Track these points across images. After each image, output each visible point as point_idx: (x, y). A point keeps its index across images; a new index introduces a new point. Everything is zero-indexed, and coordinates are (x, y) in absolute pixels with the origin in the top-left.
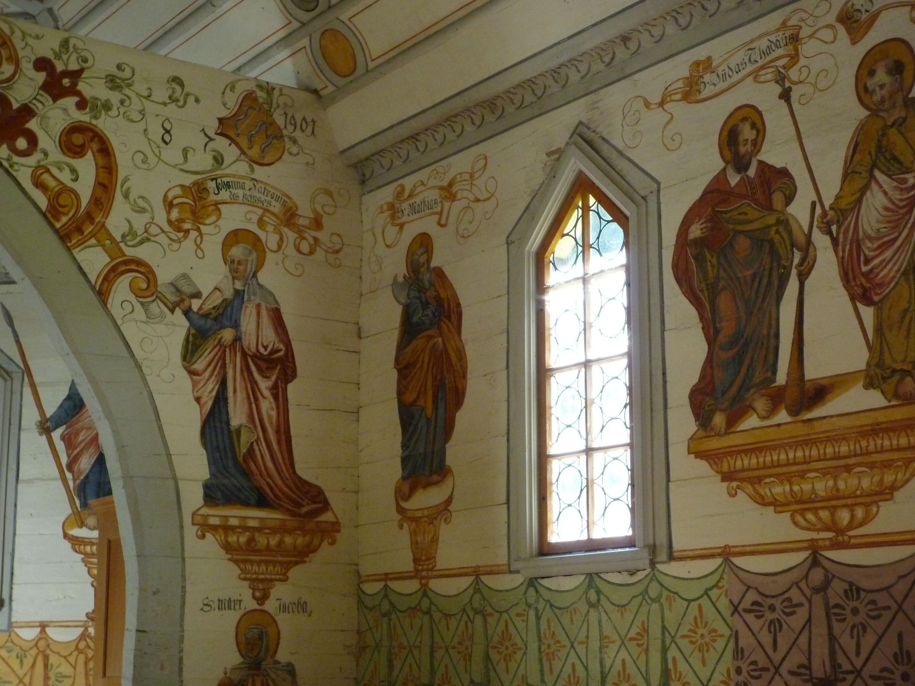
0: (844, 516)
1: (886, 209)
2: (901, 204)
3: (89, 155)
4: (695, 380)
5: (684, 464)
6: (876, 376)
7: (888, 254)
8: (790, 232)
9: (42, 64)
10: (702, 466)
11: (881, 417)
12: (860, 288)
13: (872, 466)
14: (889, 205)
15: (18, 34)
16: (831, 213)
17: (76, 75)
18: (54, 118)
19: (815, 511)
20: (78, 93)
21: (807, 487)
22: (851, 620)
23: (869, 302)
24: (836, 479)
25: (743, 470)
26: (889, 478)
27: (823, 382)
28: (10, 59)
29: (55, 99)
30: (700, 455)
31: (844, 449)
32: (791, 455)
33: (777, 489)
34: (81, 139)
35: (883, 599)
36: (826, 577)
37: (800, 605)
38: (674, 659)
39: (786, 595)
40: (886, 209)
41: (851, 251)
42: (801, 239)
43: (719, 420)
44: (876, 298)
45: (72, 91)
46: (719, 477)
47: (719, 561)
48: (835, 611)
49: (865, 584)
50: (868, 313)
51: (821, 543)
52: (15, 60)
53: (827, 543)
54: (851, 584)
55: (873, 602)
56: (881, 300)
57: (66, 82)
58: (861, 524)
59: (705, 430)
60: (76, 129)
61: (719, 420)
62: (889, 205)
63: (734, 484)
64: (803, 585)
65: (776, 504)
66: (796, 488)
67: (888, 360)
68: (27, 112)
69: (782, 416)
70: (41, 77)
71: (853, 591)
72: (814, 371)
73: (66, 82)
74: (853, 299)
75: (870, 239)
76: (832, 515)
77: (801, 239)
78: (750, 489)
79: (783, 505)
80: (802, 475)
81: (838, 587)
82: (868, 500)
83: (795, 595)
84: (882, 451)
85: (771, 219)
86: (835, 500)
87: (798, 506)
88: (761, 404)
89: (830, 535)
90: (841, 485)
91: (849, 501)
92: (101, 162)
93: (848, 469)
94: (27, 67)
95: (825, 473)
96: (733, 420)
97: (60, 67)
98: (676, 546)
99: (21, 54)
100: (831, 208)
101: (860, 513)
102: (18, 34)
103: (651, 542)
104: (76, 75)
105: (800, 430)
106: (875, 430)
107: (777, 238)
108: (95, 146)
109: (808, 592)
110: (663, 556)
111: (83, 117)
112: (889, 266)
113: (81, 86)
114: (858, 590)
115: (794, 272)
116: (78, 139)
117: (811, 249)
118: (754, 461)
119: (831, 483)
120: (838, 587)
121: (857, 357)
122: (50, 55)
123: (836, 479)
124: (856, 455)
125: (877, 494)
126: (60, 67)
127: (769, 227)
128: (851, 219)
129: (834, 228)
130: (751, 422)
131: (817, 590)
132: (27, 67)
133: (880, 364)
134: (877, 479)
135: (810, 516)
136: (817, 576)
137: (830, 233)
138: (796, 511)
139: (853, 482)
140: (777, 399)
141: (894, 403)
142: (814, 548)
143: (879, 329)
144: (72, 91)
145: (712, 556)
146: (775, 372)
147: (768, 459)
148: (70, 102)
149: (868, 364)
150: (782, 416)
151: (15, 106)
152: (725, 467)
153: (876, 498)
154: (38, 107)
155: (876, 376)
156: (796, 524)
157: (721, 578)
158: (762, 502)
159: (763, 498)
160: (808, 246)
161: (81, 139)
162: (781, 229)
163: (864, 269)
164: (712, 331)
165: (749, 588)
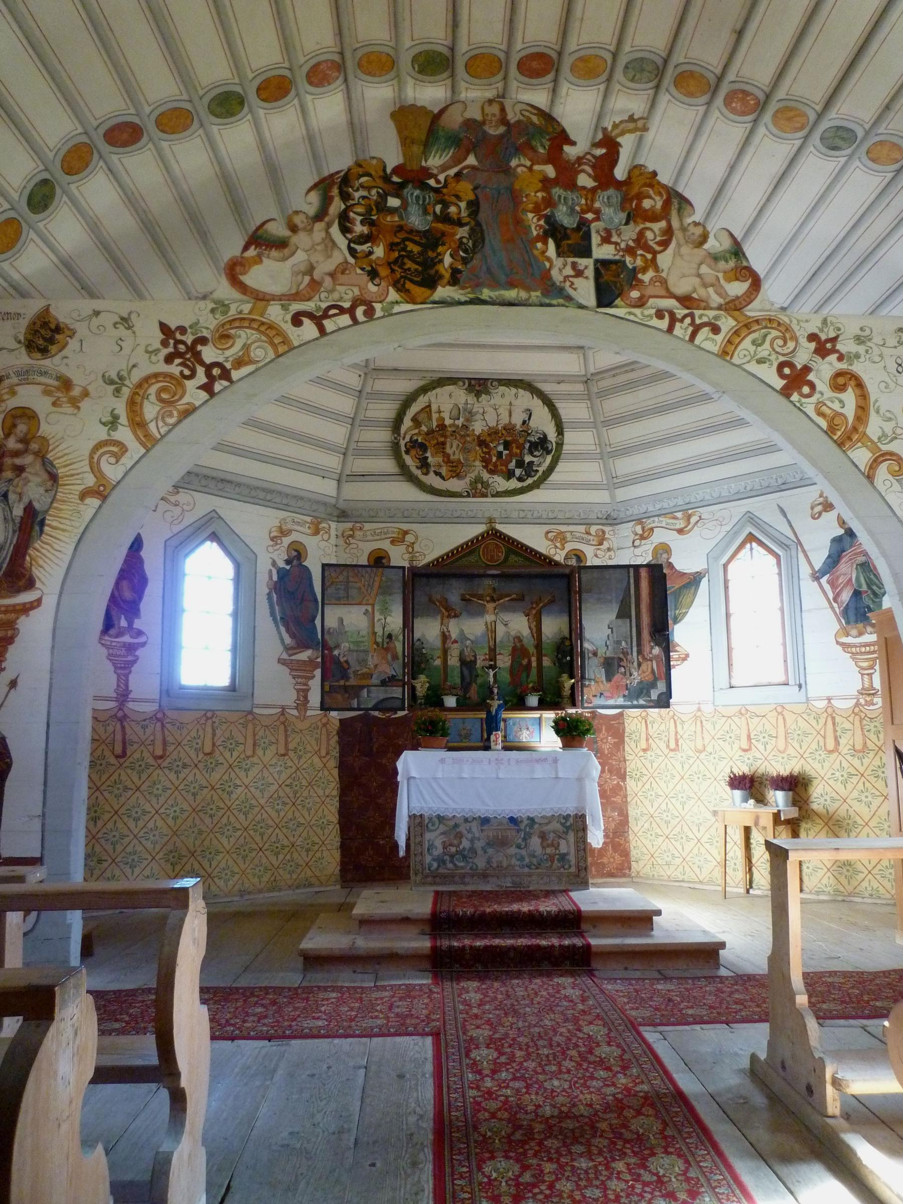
3: (850, 390)
9: (812, 337)
15: (795, 322)
17: (834, 340)
18: (824, 371)
20: (837, 351)
28: (791, 338)
29: (823, 358)
34: (844, 380)
45: (834, 351)
52: (795, 338)
57: (829, 346)
60: (839, 374)
68: (807, 369)
70: (813, 345)
73: (829, 346)
92: (858, 392)
94: (803, 341)
97: (823, 337)
99: (798, 334)
102: (795, 322)
104: (834, 340)
108: (853, 383)
111: (843, 366)
113: (838, 347)
116: (841, 380)
122: (816, 331)
126: (823, 337)
132: (803, 341)
144: (834, 351)
148: (833, 358)
151: (799, 367)
154: (813, 365)
161: (844, 380)
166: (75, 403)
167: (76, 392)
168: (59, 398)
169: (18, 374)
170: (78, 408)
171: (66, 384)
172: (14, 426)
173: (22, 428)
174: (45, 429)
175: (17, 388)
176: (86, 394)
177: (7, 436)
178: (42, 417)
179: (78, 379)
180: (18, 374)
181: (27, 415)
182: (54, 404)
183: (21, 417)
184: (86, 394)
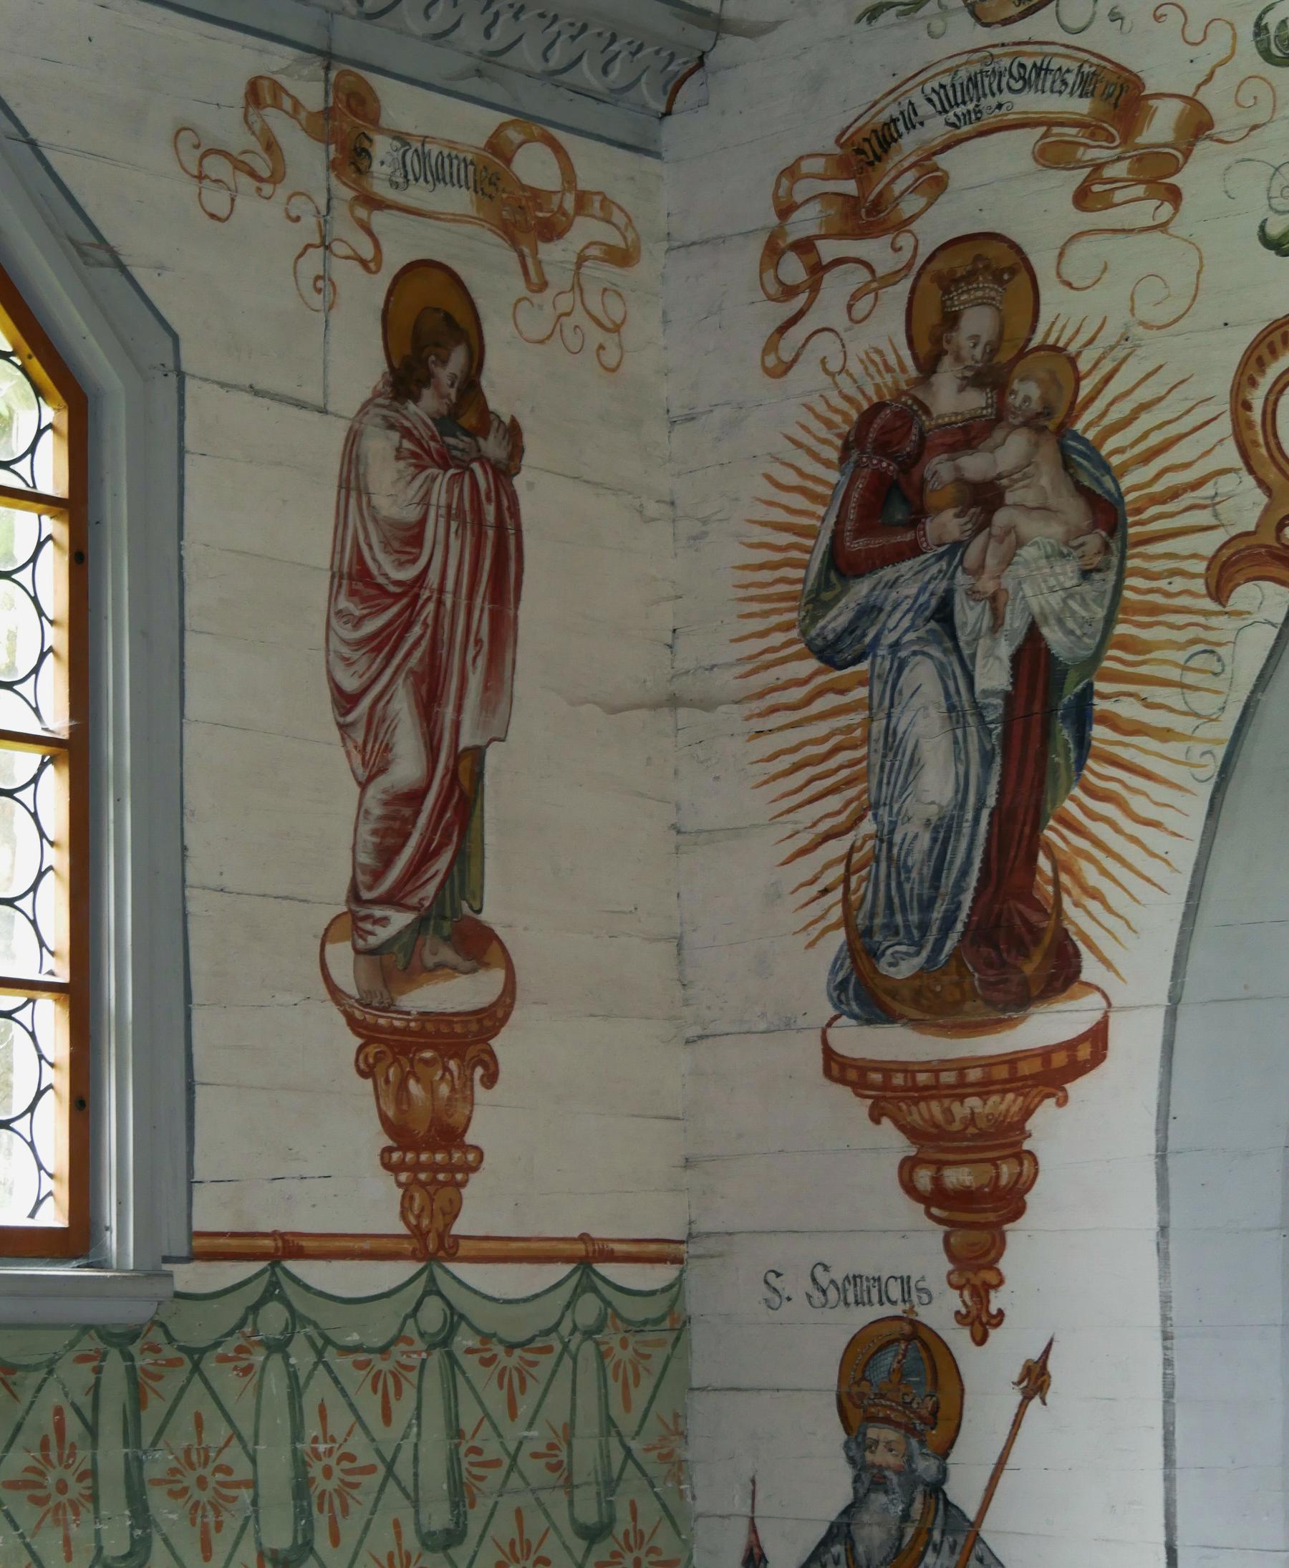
166: (1159, 175)
167: (1160, 127)
168: (1098, 167)
169: (944, 101)
170: (1174, 195)
171: (1121, 97)
172: (951, 320)
173: (977, 322)
174: (1063, 315)
175: (943, 161)
176: (1198, 125)
177: (928, 367)
178: (1043, 263)
179: (1163, 67)
180: (944, 101)
181: (991, 264)
182: (1083, 198)
183: (970, 276)
184: (1198, 125)
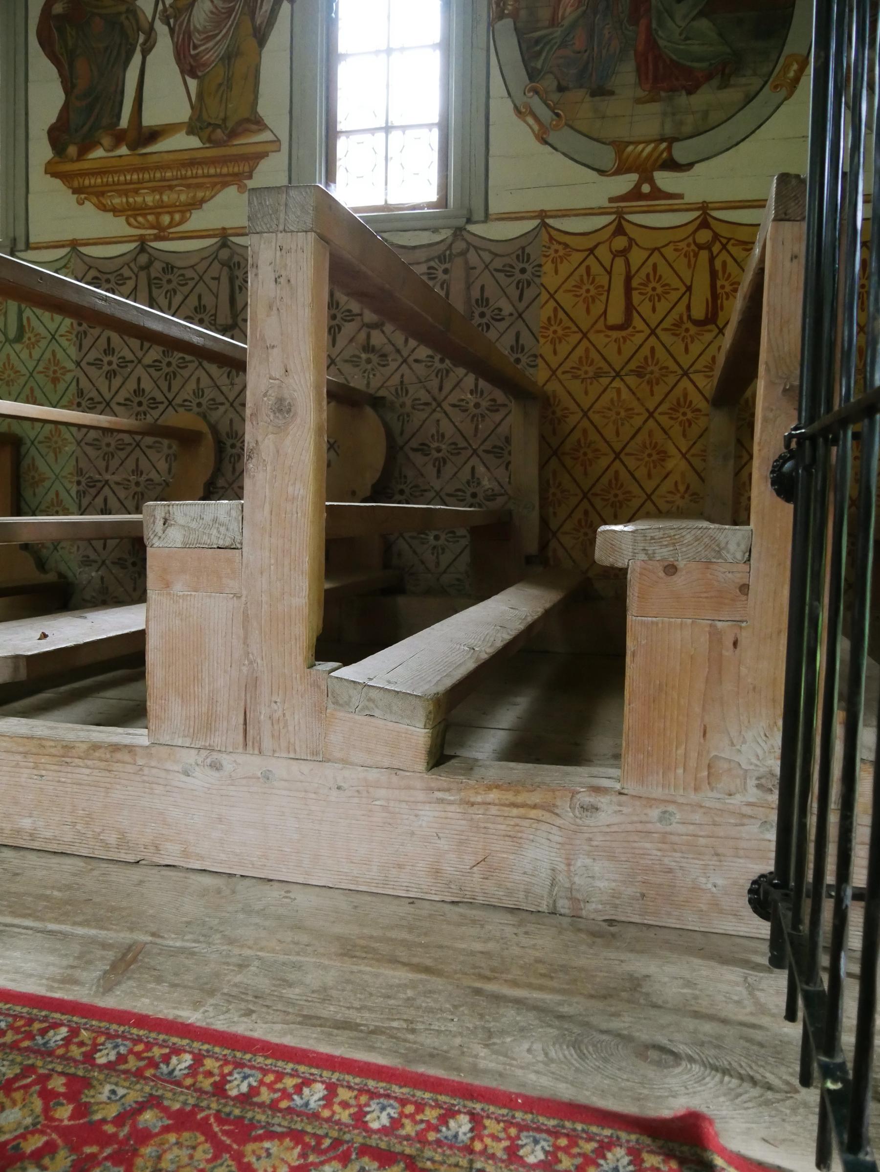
0: (166, 219)
1: (212, 12)
2: (223, 11)
4: (54, 120)
5: (39, 180)
6: (196, 126)
7: (210, 44)
8: (137, 21)
10: (57, 182)
11: (198, 155)
12: (188, 65)
13: (188, 186)
14: (214, 10)
16: (170, 11)
19: (144, 216)
21: (139, 199)
22: (167, 287)
23: (194, 75)
24: (161, 194)
25: (90, 186)
26: (200, 194)
27: (156, 128)
30: (55, 175)
31: (169, 174)
32: (128, 177)
33: (117, 201)
35: (189, 273)
36: (150, 259)
37: (130, 278)
38: (28, 319)
39: (118, 273)
40: (212, 12)
41: (183, 39)
42: (146, 26)
43: (72, 150)
44: (200, 74)
46: (70, 191)
47: (67, 250)
48: (155, 281)
49: (179, 264)
50: (193, 84)
51: (147, 237)
53: (152, 237)
54: (167, 264)
55: (183, 275)
56: (205, 75)
58: (178, 224)
59: (60, 157)
61: (72, 150)
62: (214, 10)
63: (83, 196)
64: (132, 265)
65: (116, 211)
66: (131, 200)
67: (205, 116)
69: (124, 150)
71: (169, 268)
72: (150, 119)
74: (182, 72)
75: (198, 32)
76: (157, 219)
77: (146, 26)
78: (95, 200)
79: (120, 211)
80: (136, 192)
81: (158, 265)
82: (184, 208)
83: (126, 272)
84: (196, 177)
85: (123, 8)
86: (160, 208)
87: (132, 212)
88: (107, 141)
89: (155, 231)
90: (165, 198)
91: (170, 210)
93: (171, 188)
95: (153, 190)
96: (85, 149)
98: (32, 239)
100: (171, 6)
101: (177, 217)
103: (12, 235)
105: (137, 161)
106: (192, 163)
107: (126, 23)
109: (136, 270)
110: (21, 245)
112: (211, 52)
114: (173, 267)
115: (138, 48)
117: (153, 34)
118: (99, 180)
119: (157, 197)
120: (158, 265)
121: (184, 113)
123: (161, 194)
124: (177, 179)
125: (190, 204)
127: (120, 14)
128: (184, 17)
129: (172, 21)
130: (99, 153)
131: (142, 268)
133: (199, 118)
134: (191, 195)
135: (140, 219)
136: (143, 259)
137: (168, 24)
138: (131, 216)
139: (174, 196)
140: (119, 138)
141: (207, 145)
142: (142, 241)
143: (200, 95)
145: (63, 246)
146: (119, 117)
147: (110, 179)
149: (190, 118)
150: (124, 150)
152: (76, 184)
153: (189, 207)
155: (196, 126)
156: (129, 224)
157: (69, 261)
158: (104, 208)
159: (104, 206)
160: (150, 32)
162: (131, 17)
163: (192, 52)
164: (69, 85)
165: (90, 268)
